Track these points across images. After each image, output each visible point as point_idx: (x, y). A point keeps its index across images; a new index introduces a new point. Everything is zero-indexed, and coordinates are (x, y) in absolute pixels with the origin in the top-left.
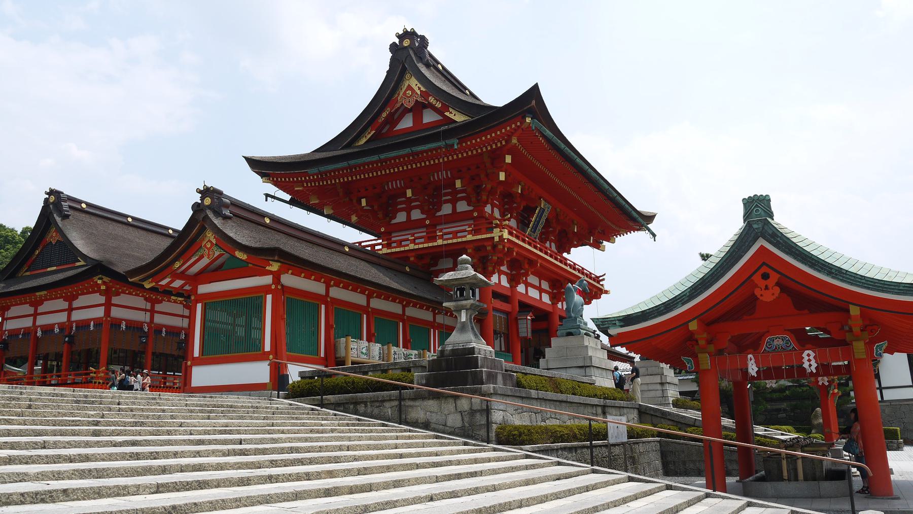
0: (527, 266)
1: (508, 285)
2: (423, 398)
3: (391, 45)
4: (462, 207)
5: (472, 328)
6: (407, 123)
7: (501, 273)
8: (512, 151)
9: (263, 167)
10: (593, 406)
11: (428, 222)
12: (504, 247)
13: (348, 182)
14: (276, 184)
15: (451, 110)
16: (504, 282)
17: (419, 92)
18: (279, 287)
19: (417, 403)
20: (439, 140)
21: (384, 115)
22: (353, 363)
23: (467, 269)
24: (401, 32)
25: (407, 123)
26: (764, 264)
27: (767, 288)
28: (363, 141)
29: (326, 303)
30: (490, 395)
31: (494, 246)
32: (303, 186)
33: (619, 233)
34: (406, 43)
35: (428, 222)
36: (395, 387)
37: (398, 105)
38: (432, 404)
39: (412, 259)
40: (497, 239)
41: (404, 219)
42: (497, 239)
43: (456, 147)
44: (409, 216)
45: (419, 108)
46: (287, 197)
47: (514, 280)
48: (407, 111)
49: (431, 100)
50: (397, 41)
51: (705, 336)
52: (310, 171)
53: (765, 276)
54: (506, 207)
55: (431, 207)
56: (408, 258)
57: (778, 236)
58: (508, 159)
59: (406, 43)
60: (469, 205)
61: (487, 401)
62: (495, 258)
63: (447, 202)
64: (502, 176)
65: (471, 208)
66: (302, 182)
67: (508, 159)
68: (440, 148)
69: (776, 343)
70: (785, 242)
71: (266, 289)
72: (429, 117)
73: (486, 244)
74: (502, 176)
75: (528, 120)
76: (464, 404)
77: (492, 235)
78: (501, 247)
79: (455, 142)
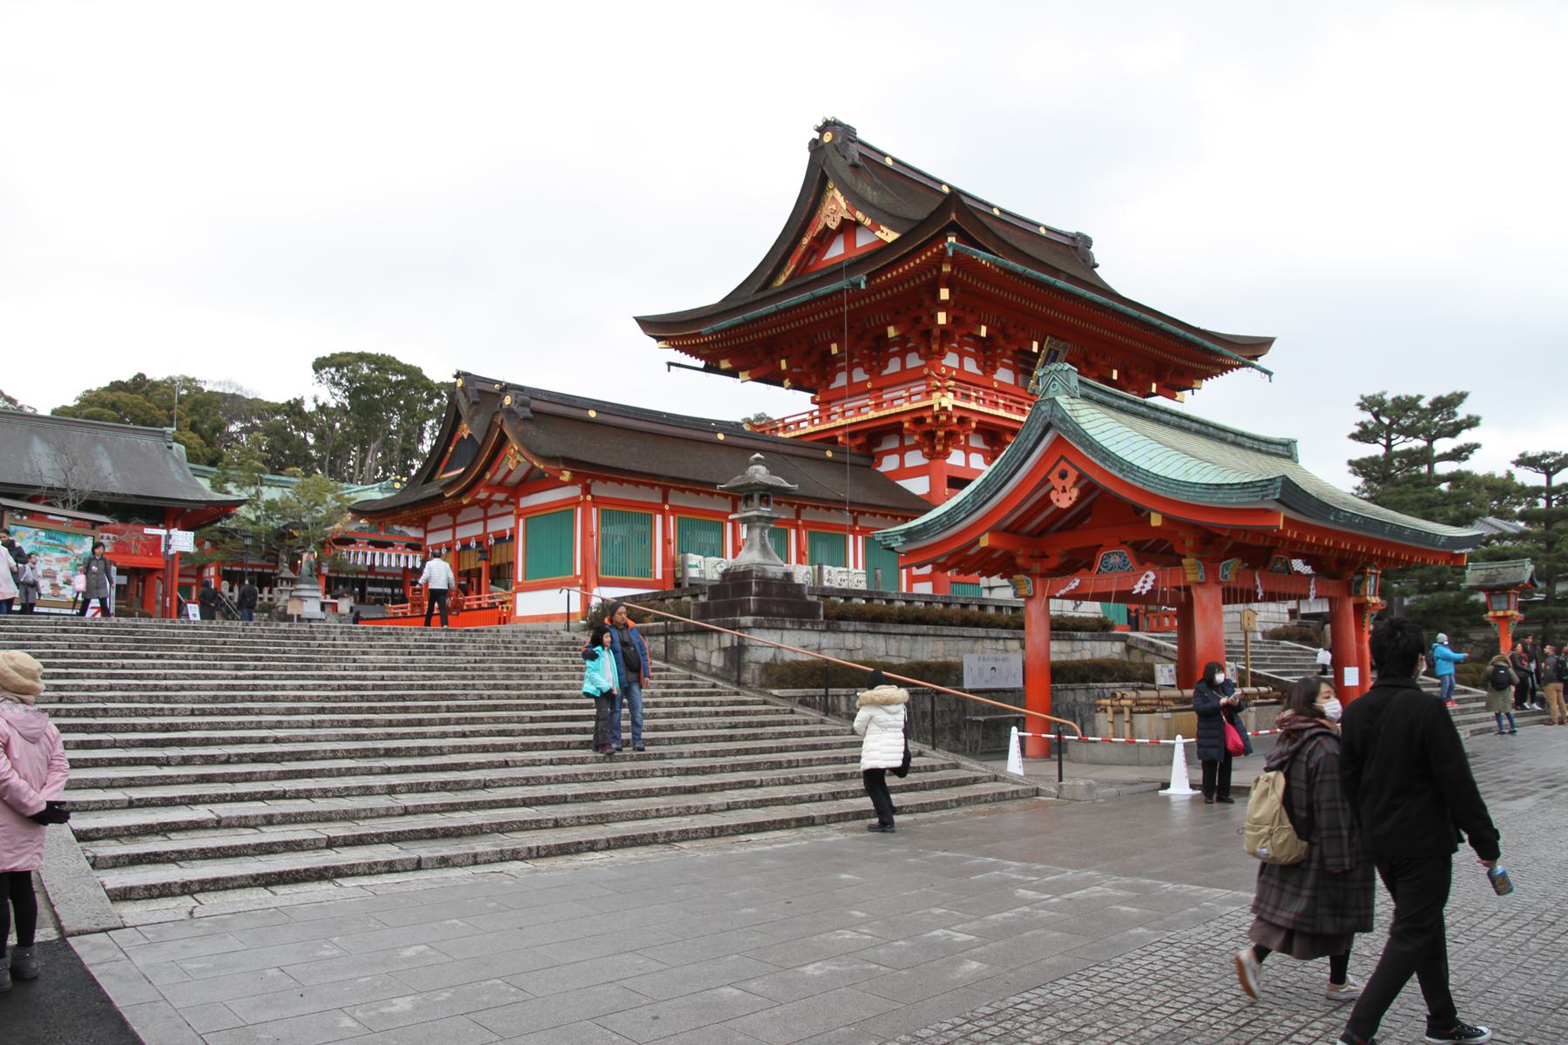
4: (913, 361)
5: (764, 546)
7: (968, 450)
8: (950, 283)
9: (661, 328)
11: (869, 385)
12: (949, 417)
17: (844, 205)
18: (589, 498)
20: (841, 279)
21: (805, 241)
25: (837, 250)
27: (1064, 491)
28: (782, 279)
30: (747, 628)
33: (1207, 375)
34: (828, 137)
35: (869, 385)
37: (820, 227)
38: (696, 640)
40: (936, 408)
42: (936, 408)
43: (863, 286)
44: (850, 378)
45: (848, 228)
46: (701, 364)
49: (859, 216)
50: (817, 135)
58: (944, 294)
59: (828, 137)
62: (941, 433)
63: (894, 355)
64: (942, 318)
67: (944, 294)
68: (841, 291)
69: (1111, 561)
71: (575, 502)
72: (863, 241)
73: (925, 414)
74: (942, 318)
75: (952, 239)
76: (727, 641)
78: (943, 418)
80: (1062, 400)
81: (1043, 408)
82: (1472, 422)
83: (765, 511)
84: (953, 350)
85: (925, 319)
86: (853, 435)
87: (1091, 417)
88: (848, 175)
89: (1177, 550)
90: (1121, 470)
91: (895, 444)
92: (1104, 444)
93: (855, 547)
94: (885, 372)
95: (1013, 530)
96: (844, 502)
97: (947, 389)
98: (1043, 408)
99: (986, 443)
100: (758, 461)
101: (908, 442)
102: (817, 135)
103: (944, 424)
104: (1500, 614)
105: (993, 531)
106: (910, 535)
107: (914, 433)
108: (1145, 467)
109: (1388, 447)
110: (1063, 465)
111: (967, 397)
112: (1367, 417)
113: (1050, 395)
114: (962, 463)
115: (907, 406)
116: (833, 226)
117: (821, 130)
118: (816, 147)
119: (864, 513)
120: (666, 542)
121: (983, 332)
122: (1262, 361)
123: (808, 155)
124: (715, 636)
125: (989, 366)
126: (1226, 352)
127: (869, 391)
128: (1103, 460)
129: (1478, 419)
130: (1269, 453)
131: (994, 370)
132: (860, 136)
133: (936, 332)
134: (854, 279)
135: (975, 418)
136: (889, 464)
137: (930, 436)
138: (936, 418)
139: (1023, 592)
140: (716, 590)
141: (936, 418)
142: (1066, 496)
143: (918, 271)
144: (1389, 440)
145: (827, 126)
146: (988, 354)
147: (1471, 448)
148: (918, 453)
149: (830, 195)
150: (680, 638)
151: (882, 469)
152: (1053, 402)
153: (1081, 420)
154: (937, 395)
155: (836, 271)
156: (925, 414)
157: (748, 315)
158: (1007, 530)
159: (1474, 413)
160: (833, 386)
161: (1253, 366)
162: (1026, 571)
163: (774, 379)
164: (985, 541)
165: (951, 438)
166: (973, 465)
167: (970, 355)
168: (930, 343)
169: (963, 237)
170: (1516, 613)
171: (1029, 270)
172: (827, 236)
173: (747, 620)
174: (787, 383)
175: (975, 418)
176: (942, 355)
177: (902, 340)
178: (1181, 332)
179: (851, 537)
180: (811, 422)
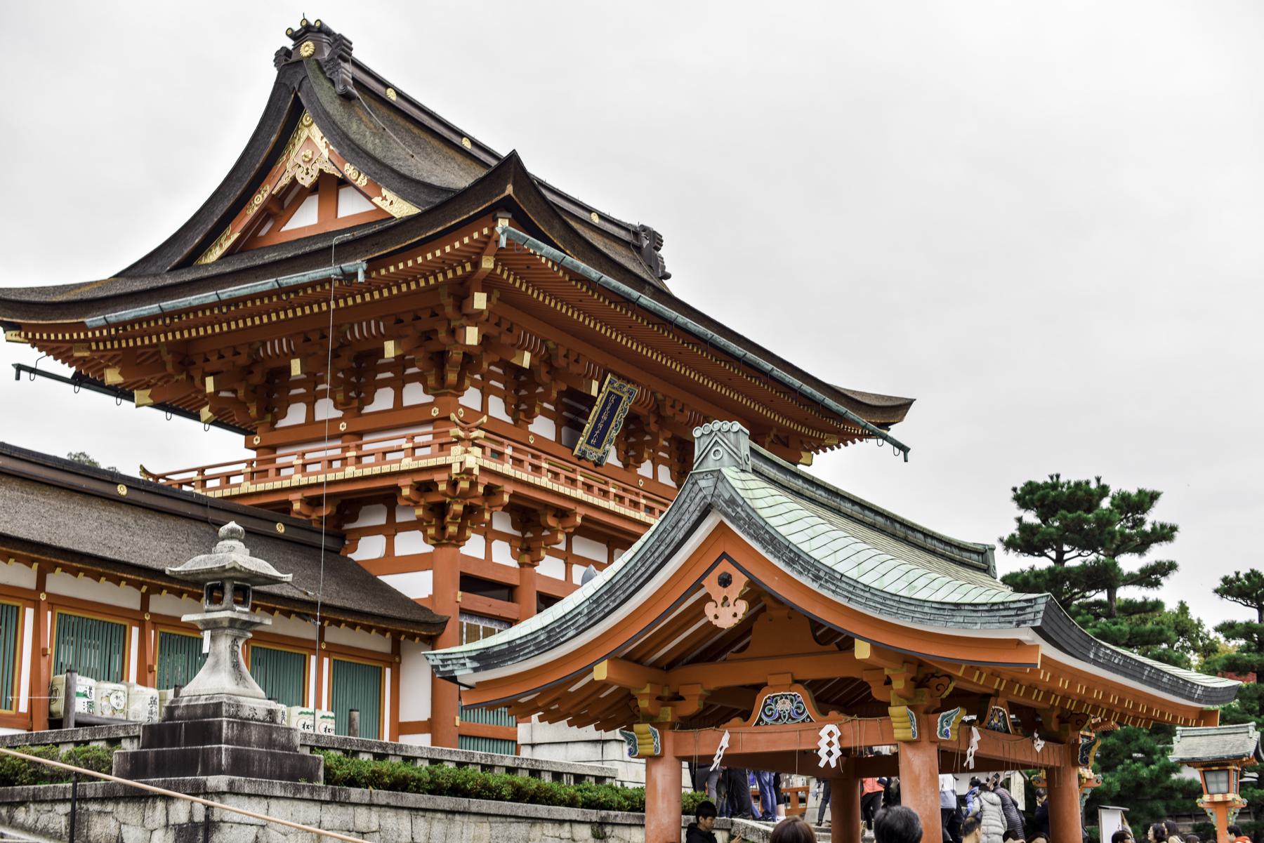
0: (551, 521)
1: (514, 563)
2: (116, 799)
3: (277, 54)
5: (236, 666)
6: (306, 218)
7: (490, 535)
8: (488, 285)
10: (562, 822)
11: (343, 427)
12: (474, 484)
13: (190, 341)
14: (34, 343)
15: (384, 192)
16: (503, 555)
17: (326, 153)
19: (109, 807)
20: (327, 263)
22: (78, 724)
23: (232, 549)
24: (297, 27)
25: (306, 218)
26: (724, 556)
29: (37, 605)
30: (219, 794)
32: (90, 348)
34: (307, 49)
36: (67, 776)
37: (285, 181)
39: (297, 506)
40: (456, 469)
41: (389, 404)
42: (456, 469)
43: (361, 278)
44: (311, 412)
45: (328, 186)
46: (68, 371)
47: (528, 551)
48: (304, 193)
49: (350, 171)
50: (289, 44)
51: (647, 690)
52: (88, 321)
53: (725, 581)
54: (523, 392)
55: (354, 393)
56: (290, 503)
57: (738, 505)
59: (307, 49)
60: (426, 391)
61: (208, 808)
62: (458, 508)
63: (385, 383)
64: (472, 336)
65: (430, 399)
66: (87, 340)
67: (480, 301)
70: (748, 515)
72: (351, 207)
73: (437, 477)
75: (503, 223)
76: (180, 813)
77: (449, 460)
78: (464, 485)
79: (359, 266)
80: (730, 473)
81: (702, 483)
82: (1165, 534)
83: (241, 612)
84: (475, 384)
85: (442, 335)
86: (314, 502)
87: (770, 501)
88: (335, 109)
89: (878, 693)
90: (816, 578)
91: (381, 520)
92: (794, 539)
93: (319, 673)
94: (368, 409)
95: (631, 658)
96: (313, 604)
98: (702, 483)
99: (514, 526)
100: (232, 535)
101: (400, 518)
102: (289, 44)
103: (464, 495)
104: (1218, 798)
105: (612, 657)
106: (486, 659)
107: (416, 504)
108: (853, 574)
109: (1059, 560)
110: (725, 567)
111: (498, 455)
112: (1031, 518)
113: (711, 464)
114: (481, 555)
115: (408, 463)
116: (307, 181)
117: (298, 37)
118: (285, 60)
119: (338, 623)
120: (38, 652)
121: (526, 360)
122: (895, 431)
123: (274, 73)
124: (160, 805)
125: (522, 411)
126: (852, 415)
127: (340, 436)
128: (790, 563)
129: (1174, 529)
130: (962, 564)
131: (530, 416)
132: (356, 54)
133: (456, 355)
134: (348, 266)
135: (509, 488)
136: (369, 549)
137: (439, 511)
138: (453, 484)
139: (649, 750)
140: (153, 734)
141: (453, 484)
142: (732, 610)
143: (445, 264)
144: (1061, 554)
145: (307, 32)
146: (522, 393)
147: (1166, 568)
148: (417, 535)
149: (304, 133)
150: (94, 807)
151: (356, 556)
152: (718, 475)
153: (757, 504)
154: (456, 450)
155: (314, 251)
156: (437, 477)
157: (168, 304)
158: (627, 657)
159: (1169, 521)
160: (282, 423)
161: (885, 438)
162: (651, 719)
163: (182, 405)
164: (601, 672)
165: (471, 516)
166: (495, 560)
167: (496, 392)
168: (443, 368)
169: (521, 220)
170: (1238, 797)
171: (606, 278)
172: (292, 196)
173: (217, 781)
174: (206, 412)
175: (509, 488)
176: (459, 389)
177: (400, 363)
178: (797, 383)
179: (313, 659)
180: (252, 476)
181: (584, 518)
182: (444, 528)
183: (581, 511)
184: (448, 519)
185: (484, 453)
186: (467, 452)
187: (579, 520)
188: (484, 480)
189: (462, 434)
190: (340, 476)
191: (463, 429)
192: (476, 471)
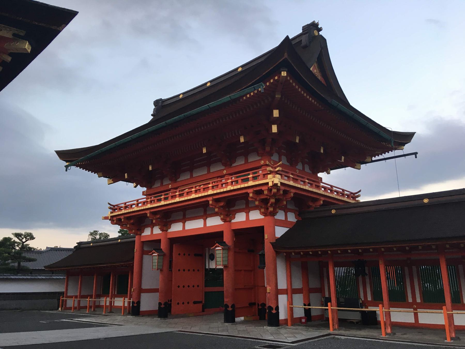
7: (286, 210)
31: (270, 190)
40: (270, 184)
42: (270, 184)
56: (208, 201)
58: (276, 113)
64: (275, 129)
67: (276, 113)
73: (264, 188)
74: (275, 129)
75: (284, 74)
78: (274, 190)
97: (277, 173)
103: (275, 194)
107: (256, 200)
114: (284, 219)
154: (270, 176)
156: (264, 188)
181: (324, 201)
182: (268, 209)
183: (323, 199)
184: (269, 205)
185: (281, 177)
186: (274, 177)
187: (322, 202)
188: (283, 188)
189: (271, 169)
190: (225, 190)
191: (272, 167)
192: (279, 185)
